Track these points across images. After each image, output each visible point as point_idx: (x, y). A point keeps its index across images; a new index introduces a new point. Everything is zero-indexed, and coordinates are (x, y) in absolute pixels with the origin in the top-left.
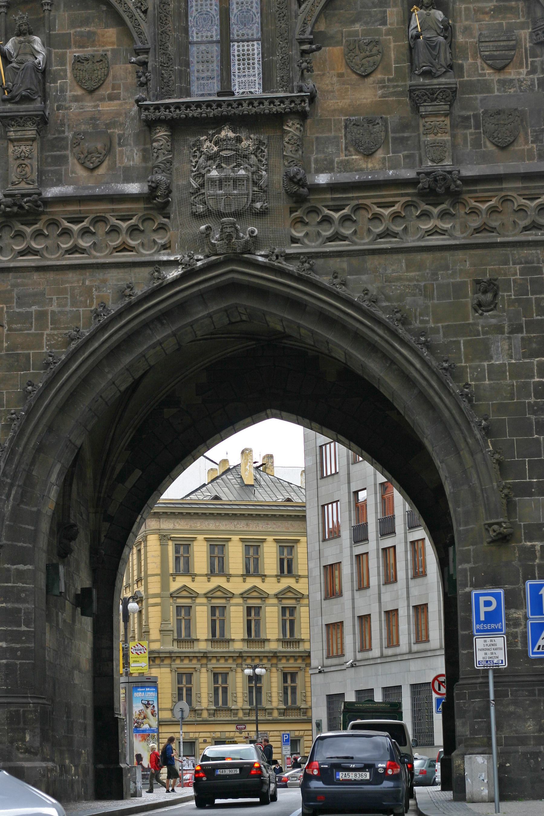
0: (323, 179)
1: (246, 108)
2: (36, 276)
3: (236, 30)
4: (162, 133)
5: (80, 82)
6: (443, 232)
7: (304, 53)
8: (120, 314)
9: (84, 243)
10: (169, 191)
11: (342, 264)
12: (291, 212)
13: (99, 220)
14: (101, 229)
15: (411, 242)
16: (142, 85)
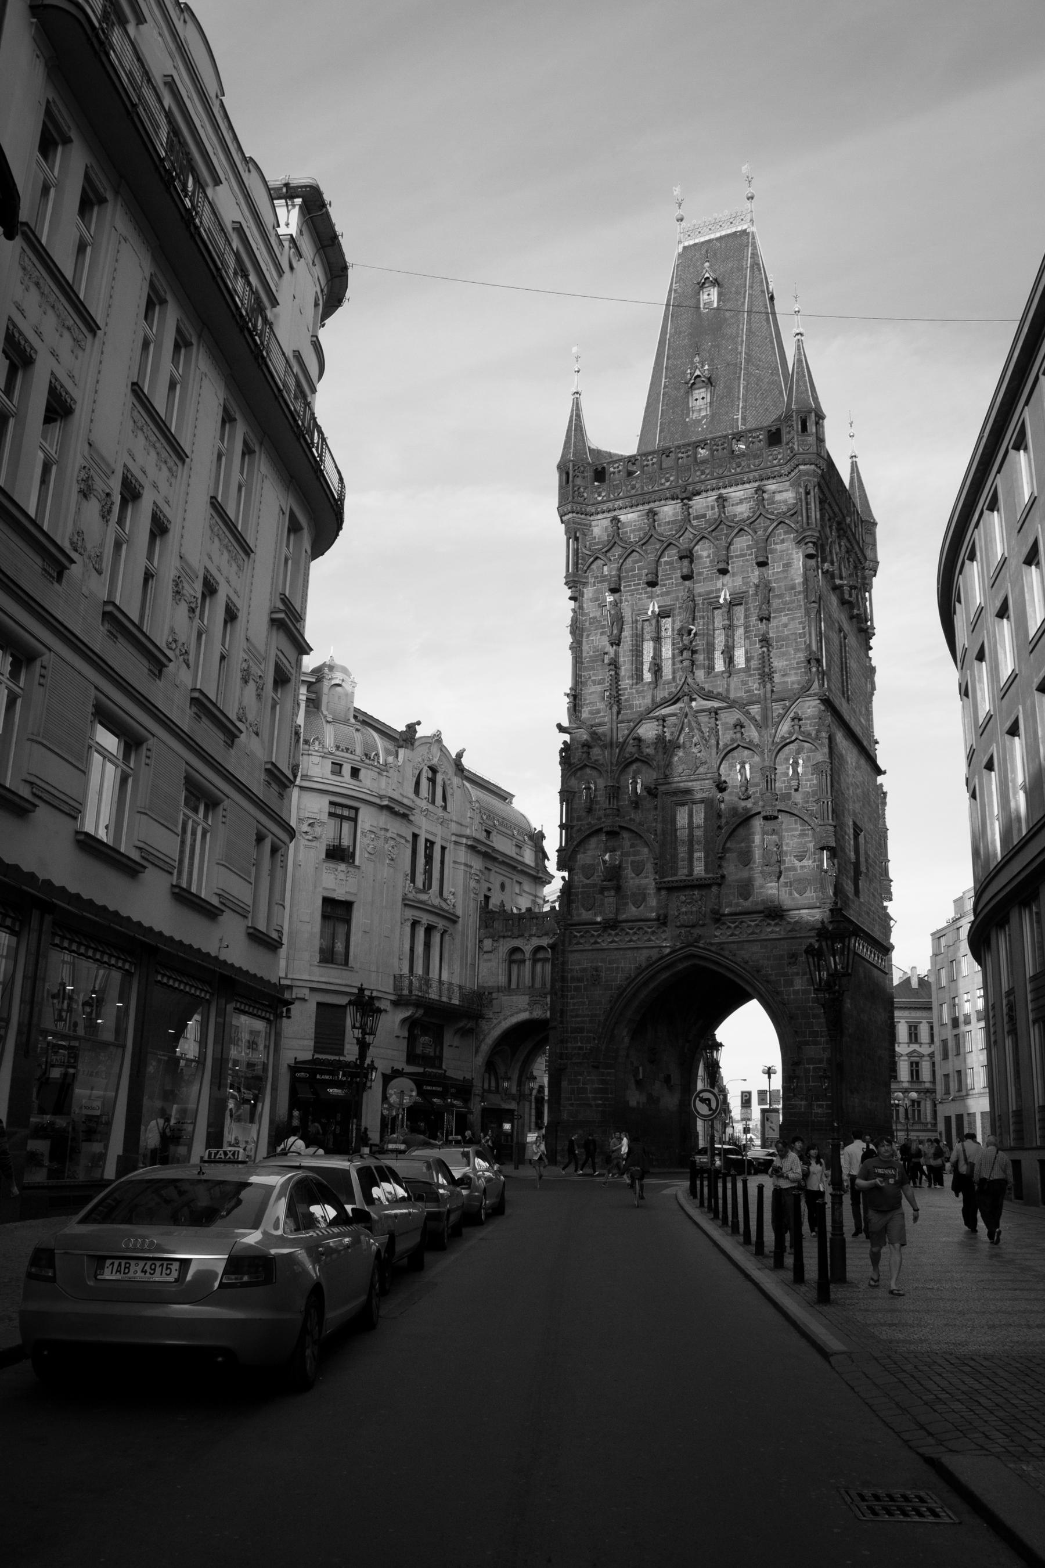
0: (727, 911)
1: (695, 882)
2: (615, 952)
3: (696, 847)
4: (663, 892)
5: (633, 871)
6: (776, 932)
7: (720, 858)
8: (647, 968)
9: (634, 938)
10: (666, 917)
11: (734, 946)
12: (715, 924)
13: (639, 929)
14: (641, 932)
15: (763, 937)
16: (656, 873)
